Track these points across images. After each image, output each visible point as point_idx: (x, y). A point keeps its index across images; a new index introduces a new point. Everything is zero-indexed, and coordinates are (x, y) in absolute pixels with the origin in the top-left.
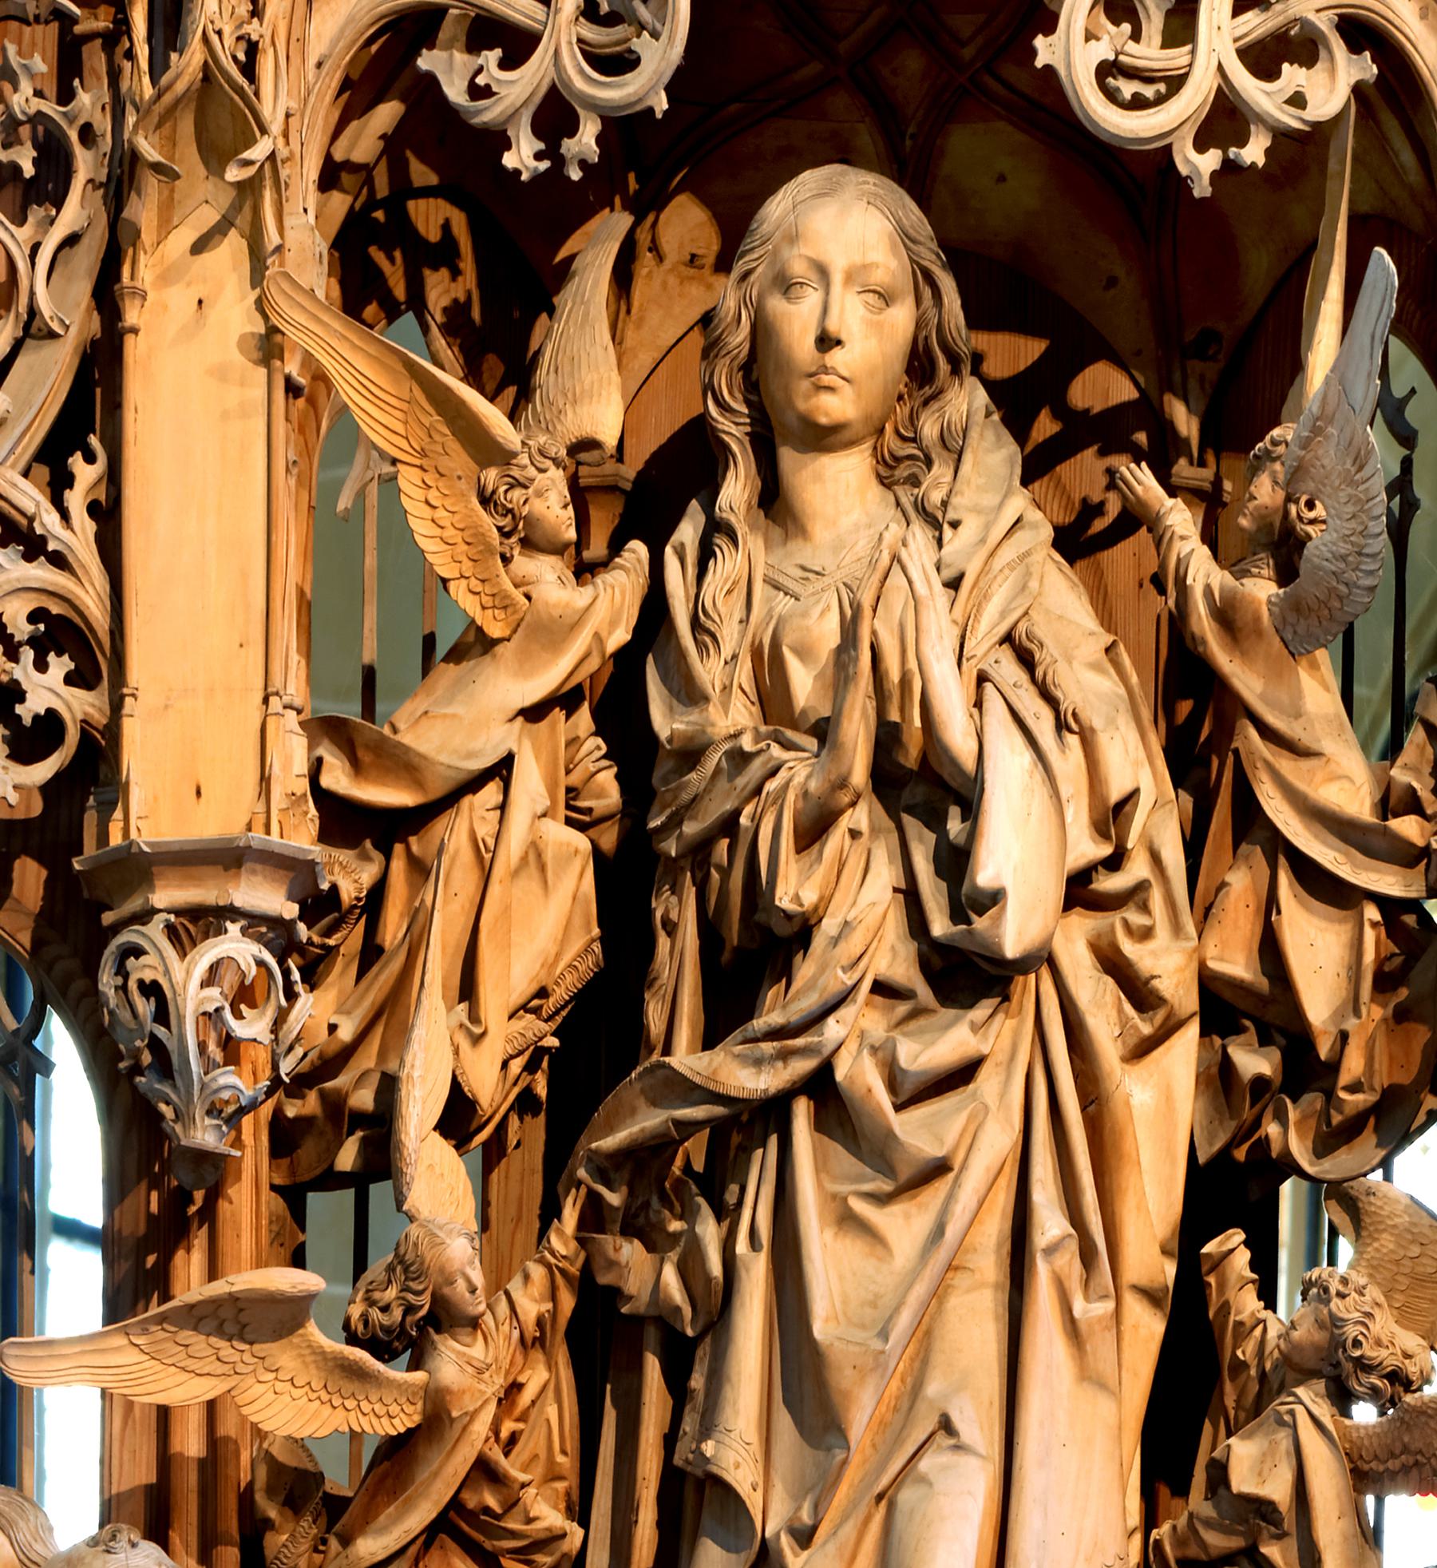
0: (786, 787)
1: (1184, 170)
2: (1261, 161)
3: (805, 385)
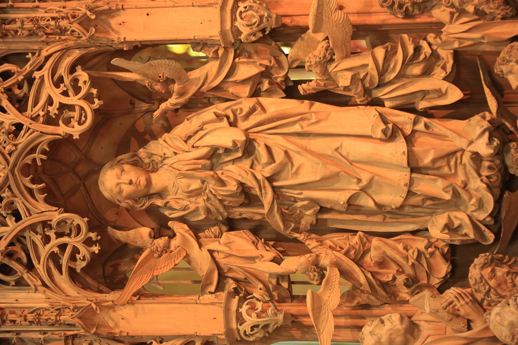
0: (213, 189)
1: (98, 106)
2: (96, 90)
3: (139, 187)
